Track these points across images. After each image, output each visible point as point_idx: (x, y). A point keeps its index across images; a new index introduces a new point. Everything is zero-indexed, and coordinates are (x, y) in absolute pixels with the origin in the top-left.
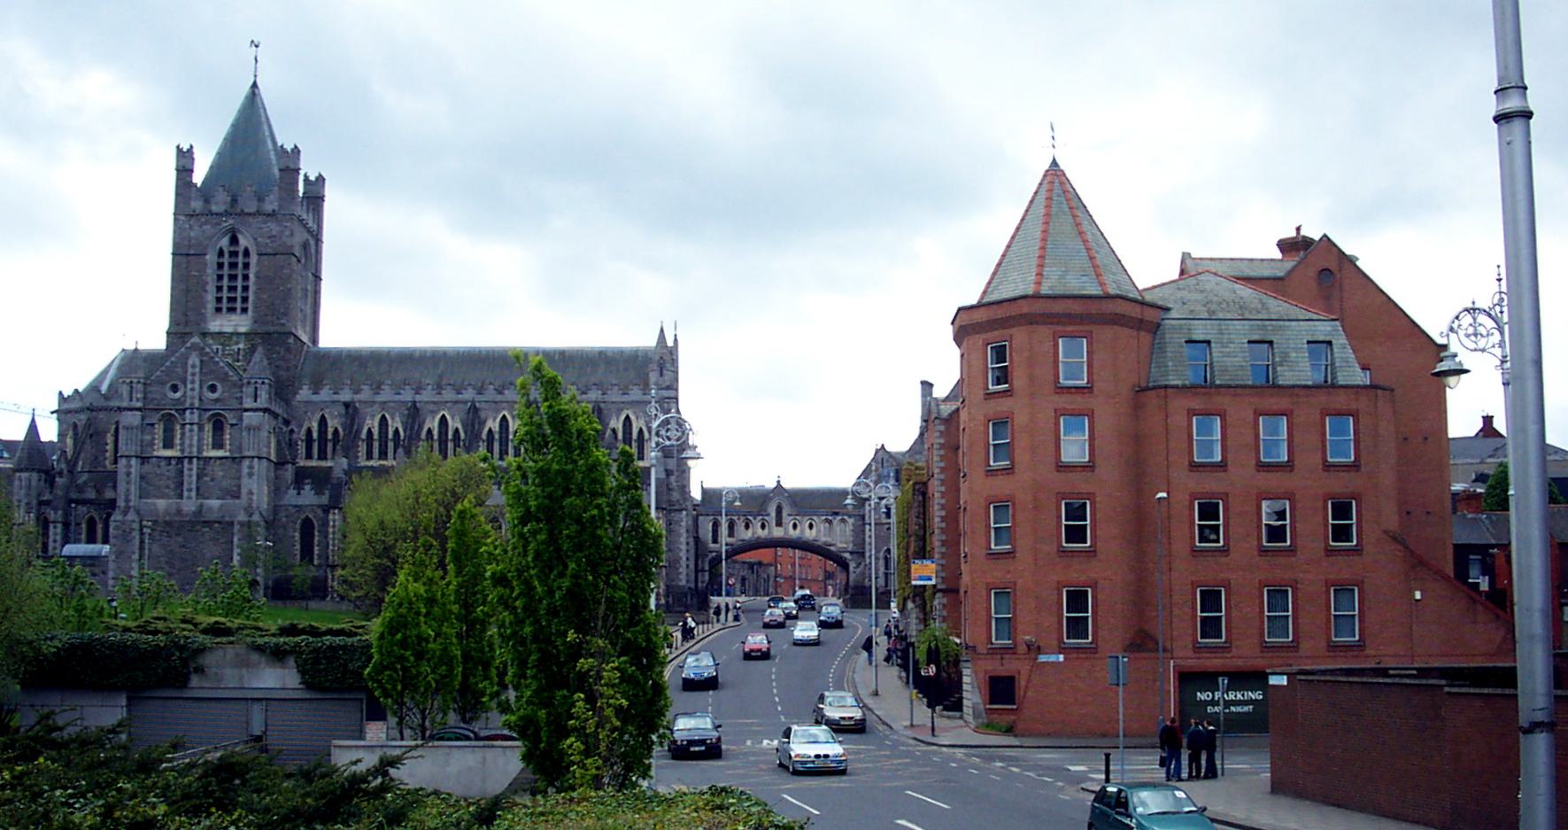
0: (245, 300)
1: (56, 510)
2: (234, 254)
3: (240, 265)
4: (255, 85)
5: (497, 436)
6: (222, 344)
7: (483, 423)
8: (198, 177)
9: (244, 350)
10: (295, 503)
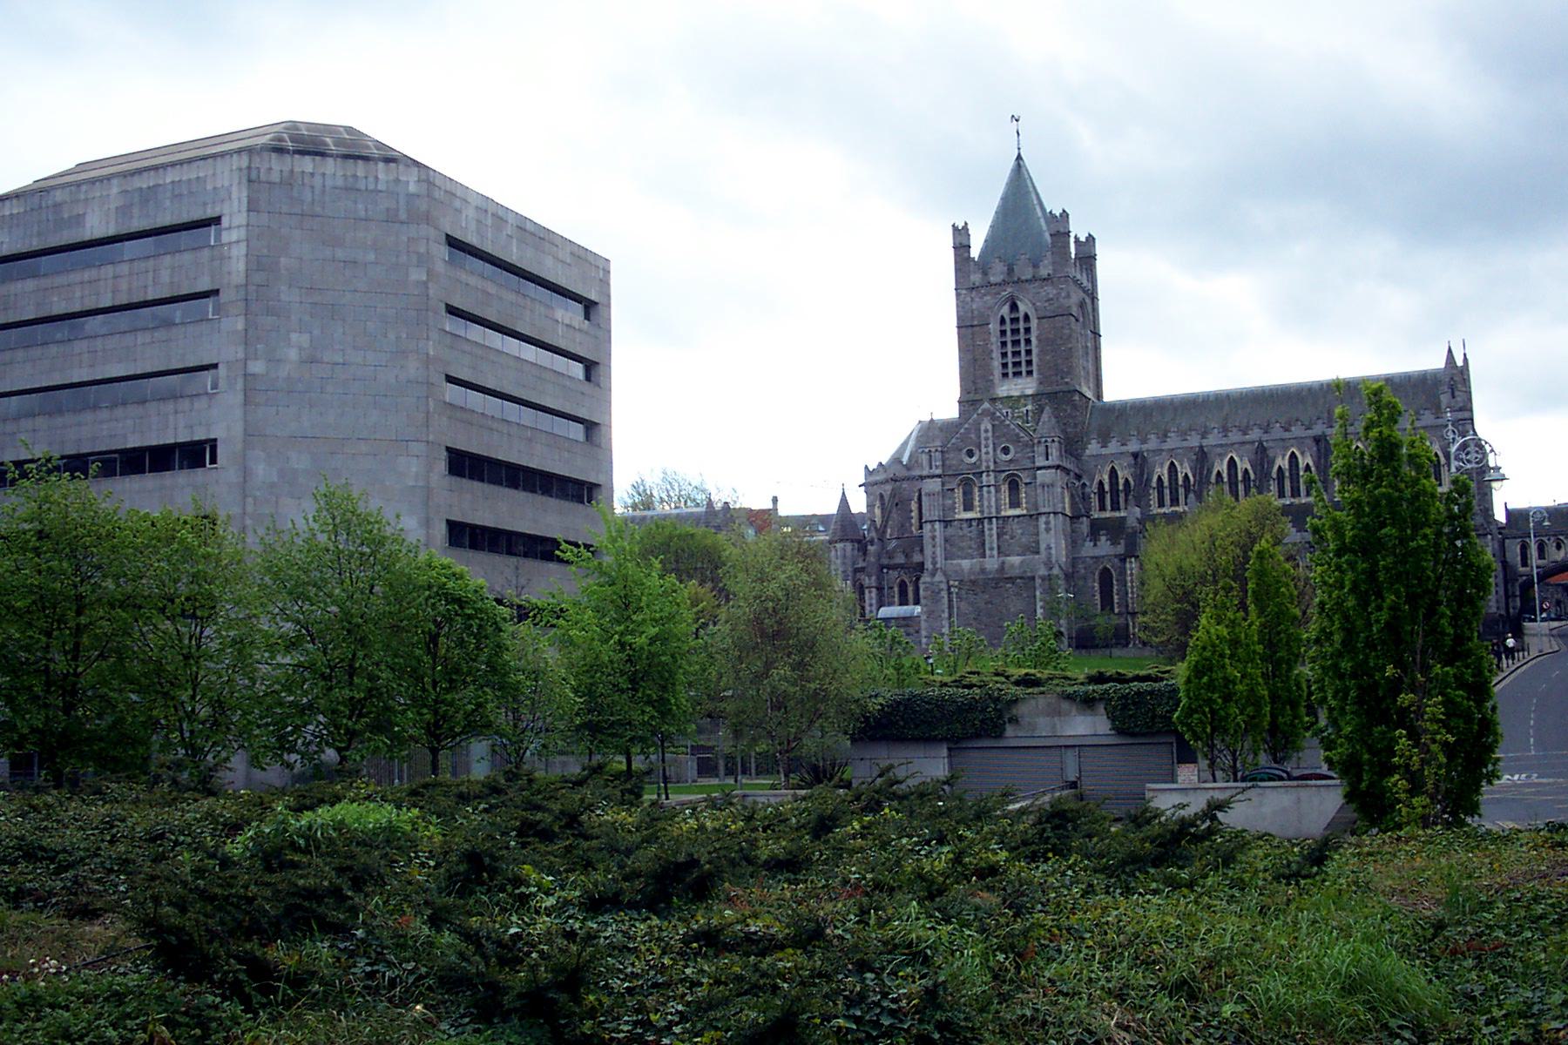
0: (1029, 363)
1: (870, 576)
2: (1015, 320)
3: (1022, 331)
4: (1019, 157)
5: (1287, 474)
6: (1011, 408)
7: (1272, 462)
8: (975, 253)
9: (1032, 411)
10: (1092, 555)
